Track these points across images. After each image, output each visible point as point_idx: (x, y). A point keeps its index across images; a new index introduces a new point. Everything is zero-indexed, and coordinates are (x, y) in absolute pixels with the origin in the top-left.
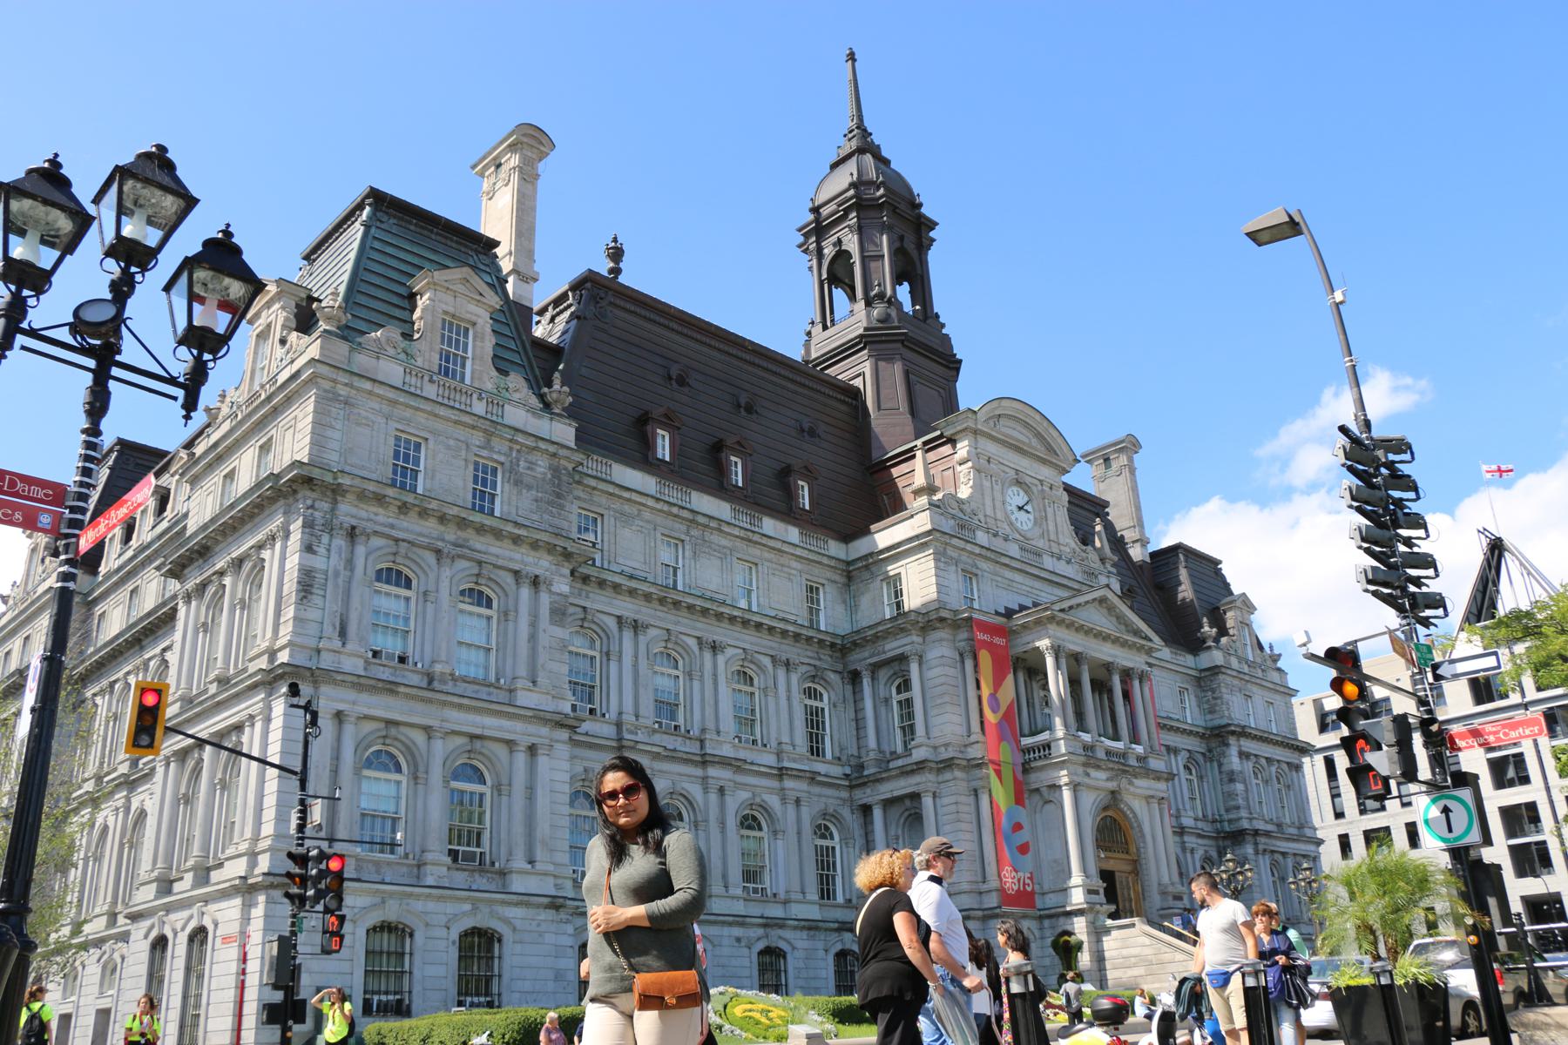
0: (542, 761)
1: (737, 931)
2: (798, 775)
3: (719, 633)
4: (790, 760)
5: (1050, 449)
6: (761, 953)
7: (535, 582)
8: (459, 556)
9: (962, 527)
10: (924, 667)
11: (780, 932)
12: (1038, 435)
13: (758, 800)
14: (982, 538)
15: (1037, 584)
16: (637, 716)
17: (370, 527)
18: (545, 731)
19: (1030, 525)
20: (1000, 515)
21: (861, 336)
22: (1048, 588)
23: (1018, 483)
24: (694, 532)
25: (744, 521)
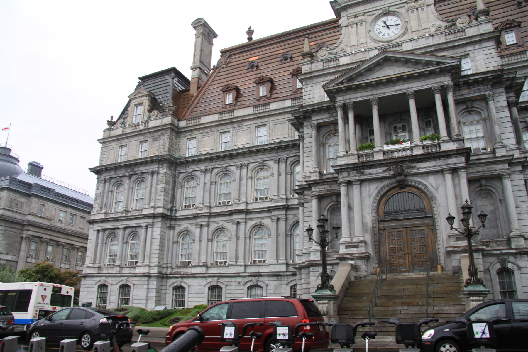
0: (150, 230)
1: (239, 279)
2: (277, 208)
3: (244, 161)
4: (275, 202)
6: (250, 288)
7: (153, 173)
8: (132, 175)
9: (329, 61)
11: (261, 279)
13: (258, 223)
16: (203, 204)
17: (108, 177)
18: (151, 220)
19: (396, 32)
23: (386, 13)
24: (235, 125)
25: (261, 109)
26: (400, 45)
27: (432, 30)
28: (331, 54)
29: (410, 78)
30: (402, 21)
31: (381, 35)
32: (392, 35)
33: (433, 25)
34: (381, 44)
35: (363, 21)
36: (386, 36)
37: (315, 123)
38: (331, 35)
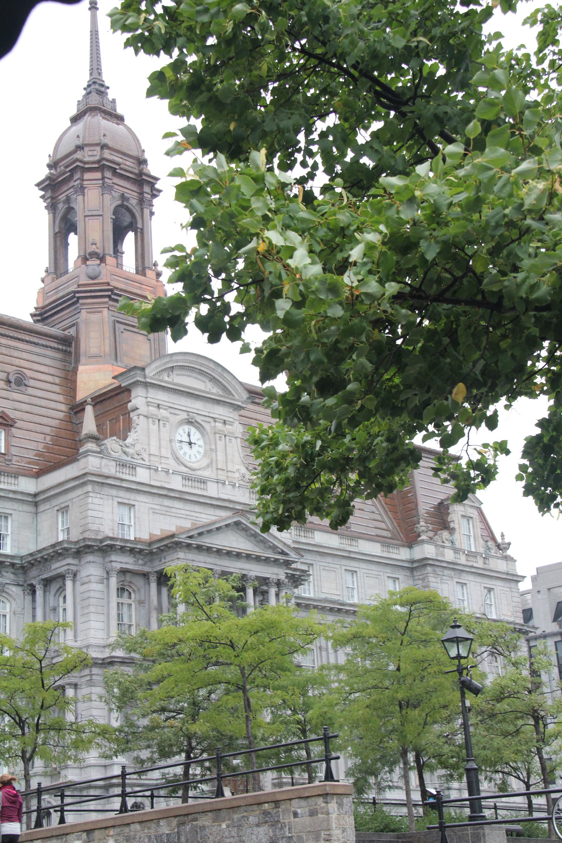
5: (225, 389)
9: (123, 465)
10: (78, 584)
12: (213, 379)
14: (142, 475)
15: (197, 508)
19: (199, 457)
20: (165, 452)
21: (75, 292)
22: (211, 511)
23: (190, 422)
26: (203, 481)
27: (237, 475)
28: (125, 453)
29: (258, 559)
30: (205, 443)
31: (181, 452)
32: (193, 459)
33: (238, 470)
34: (183, 469)
35: (167, 420)
36: (187, 458)
37: (118, 566)
38: (25, 356)
